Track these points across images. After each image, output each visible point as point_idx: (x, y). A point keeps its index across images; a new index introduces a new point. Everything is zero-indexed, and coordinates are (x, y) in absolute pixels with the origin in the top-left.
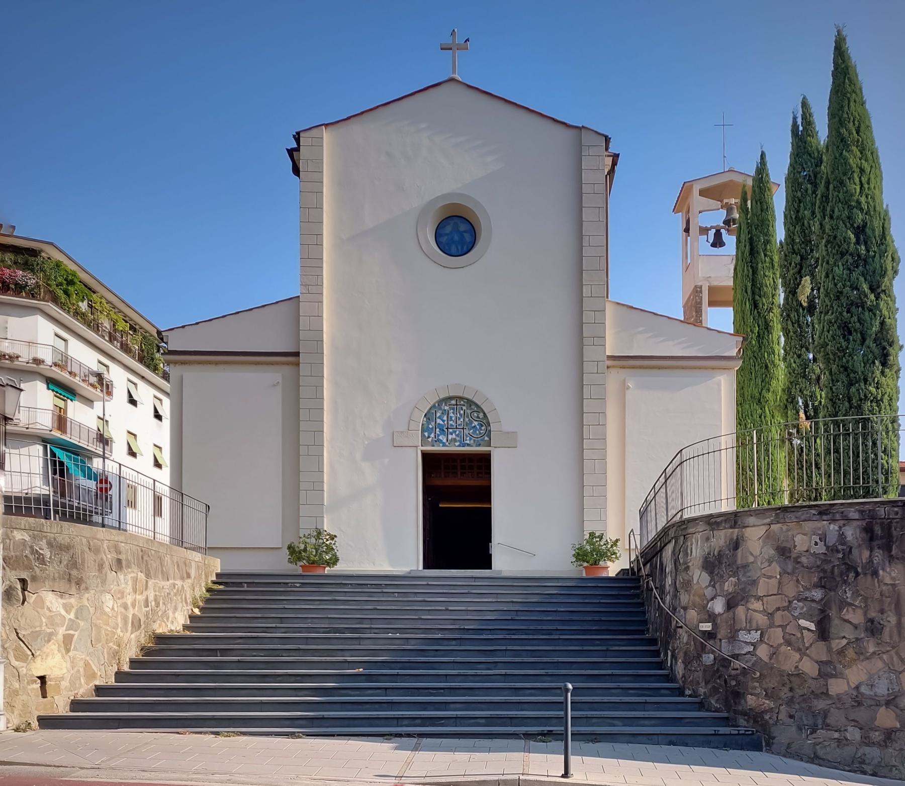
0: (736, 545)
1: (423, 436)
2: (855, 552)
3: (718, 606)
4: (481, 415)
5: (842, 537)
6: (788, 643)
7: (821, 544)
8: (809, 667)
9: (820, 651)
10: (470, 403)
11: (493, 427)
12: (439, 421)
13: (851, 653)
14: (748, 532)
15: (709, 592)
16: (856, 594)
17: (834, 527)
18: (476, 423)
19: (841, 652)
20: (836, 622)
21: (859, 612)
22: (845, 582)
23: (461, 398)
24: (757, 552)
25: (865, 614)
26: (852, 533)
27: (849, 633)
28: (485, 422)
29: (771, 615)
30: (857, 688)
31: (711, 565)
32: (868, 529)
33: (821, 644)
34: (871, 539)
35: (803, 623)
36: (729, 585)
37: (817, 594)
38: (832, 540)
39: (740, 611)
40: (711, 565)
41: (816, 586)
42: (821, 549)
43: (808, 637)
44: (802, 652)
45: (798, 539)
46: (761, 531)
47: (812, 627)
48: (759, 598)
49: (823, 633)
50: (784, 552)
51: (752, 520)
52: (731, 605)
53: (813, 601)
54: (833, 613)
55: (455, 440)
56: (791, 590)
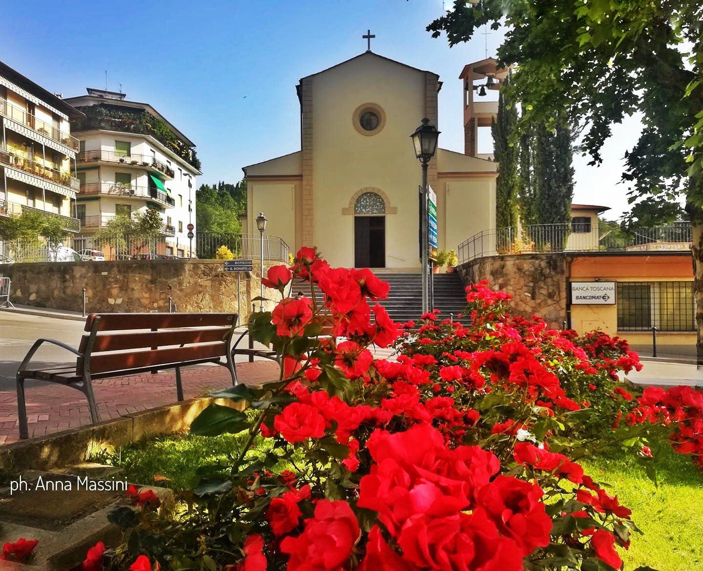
0: (503, 267)
1: (355, 209)
2: (544, 271)
3: (496, 288)
4: (381, 200)
5: (540, 265)
6: (521, 301)
7: (533, 267)
8: (529, 309)
9: (532, 303)
10: (376, 195)
11: (386, 205)
12: (362, 203)
13: (542, 304)
14: (507, 263)
15: (493, 283)
16: (545, 284)
17: (537, 262)
18: (378, 204)
19: (539, 304)
20: (537, 293)
21: (546, 290)
22: (541, 280)
23: (372, 193)
24: (510, 270)
25: (548, 290)
26: (543, 264)
27: (542, 298)
28: (383, 203)
29: (515, 292)
30: (545, 316)
31: (494, 273)
32: (548, 263)
33: (532, 301)
34: (550, 266)
35: (526, 294)
36: (500, 281)
37: (531, 284)
38: (537, 266)
39: (504, 289)
40: (494, 273)
41: (531, 281)
42: (533, 269)
43: (528, 299)
44: (526, 303)
45: (525, 265)
46: (512, 263)
47: (530, 295)
48: (511, 285)
49: (533, 298)
50: (520, 269)
51: (509, 259)
52: (501, 287)
53: (530, 287)
54: (537, 291)
55: (369, 211)
56: (522, 283)
